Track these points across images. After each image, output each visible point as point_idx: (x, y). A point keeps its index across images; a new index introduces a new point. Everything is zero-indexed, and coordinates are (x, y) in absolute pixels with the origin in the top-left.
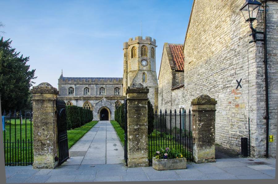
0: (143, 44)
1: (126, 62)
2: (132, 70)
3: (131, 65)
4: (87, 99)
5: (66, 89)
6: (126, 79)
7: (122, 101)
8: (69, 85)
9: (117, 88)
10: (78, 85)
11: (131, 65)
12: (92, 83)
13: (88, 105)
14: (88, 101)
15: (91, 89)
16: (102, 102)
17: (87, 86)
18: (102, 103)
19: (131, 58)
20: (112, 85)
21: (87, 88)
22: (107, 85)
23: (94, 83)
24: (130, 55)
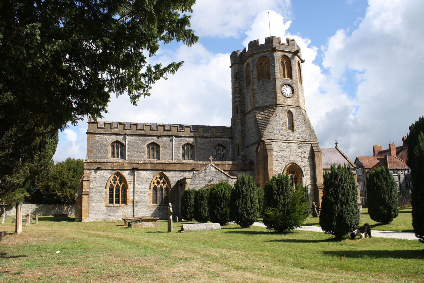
0: (283, 53)
1: (240, 90)
2: (261, 103)
3: (257, 95)
4: (160, 167)
5: (105, 146)
6: (242, 125)
7: (239, 173)
8: (114, 136)
9: (220, 145)
10: (134, 137)
11: (257, 95)
12: (165, 133)
13: (164, 183)
14: (165, 173)
15: (163, 147)
16: (205, 173)
17: (154, 139)
18: (205, 176)
19: (256, 80)
20: (208, 140)
21: (153, 143)
22: (198, 139)
23: (170, 133)
24: (254, 74)
